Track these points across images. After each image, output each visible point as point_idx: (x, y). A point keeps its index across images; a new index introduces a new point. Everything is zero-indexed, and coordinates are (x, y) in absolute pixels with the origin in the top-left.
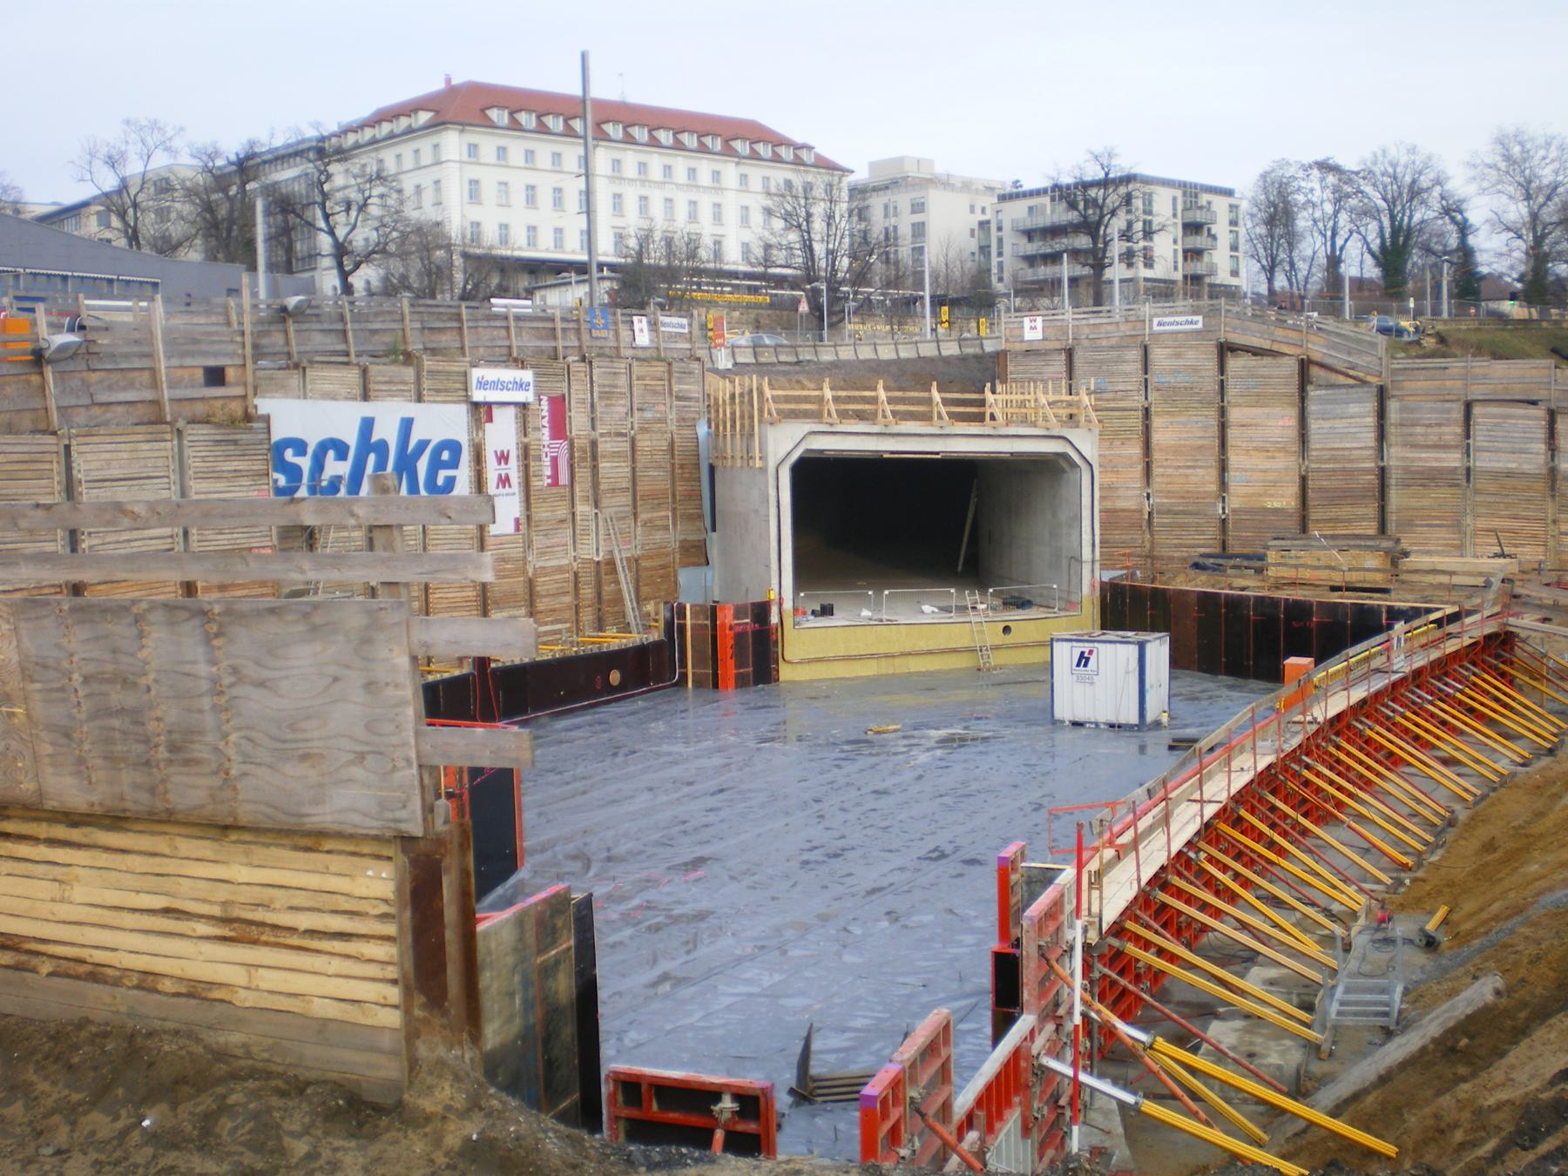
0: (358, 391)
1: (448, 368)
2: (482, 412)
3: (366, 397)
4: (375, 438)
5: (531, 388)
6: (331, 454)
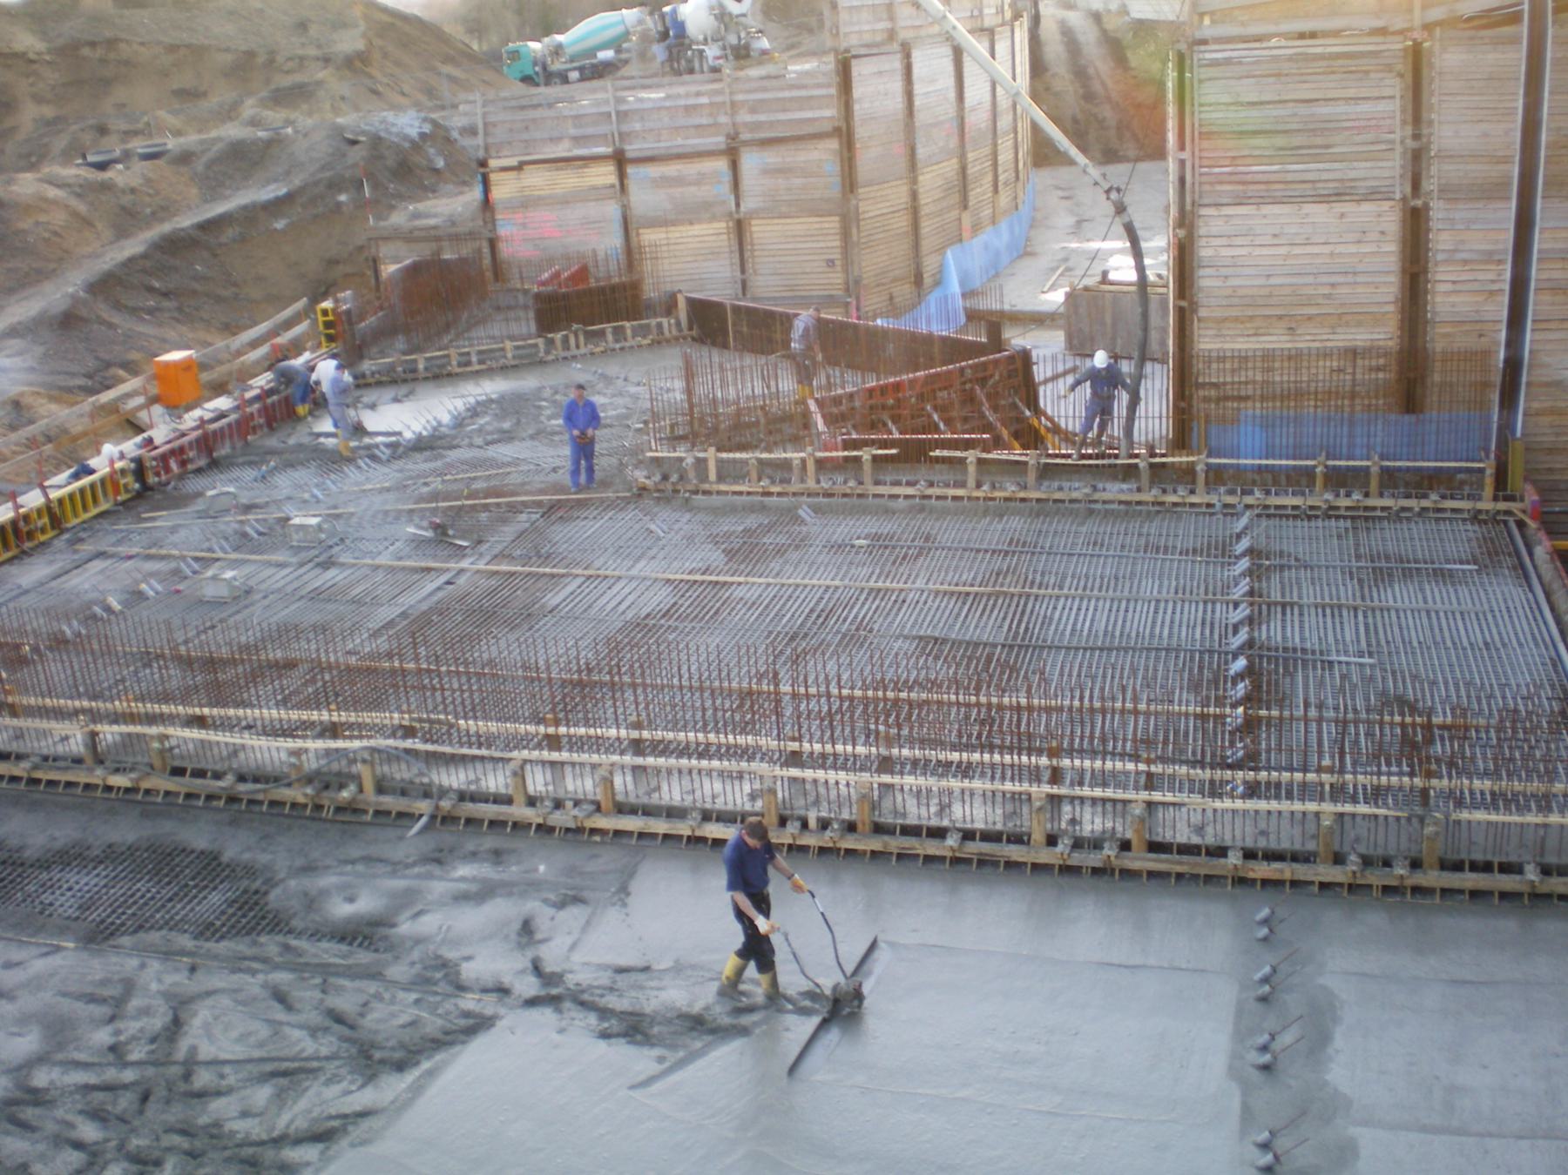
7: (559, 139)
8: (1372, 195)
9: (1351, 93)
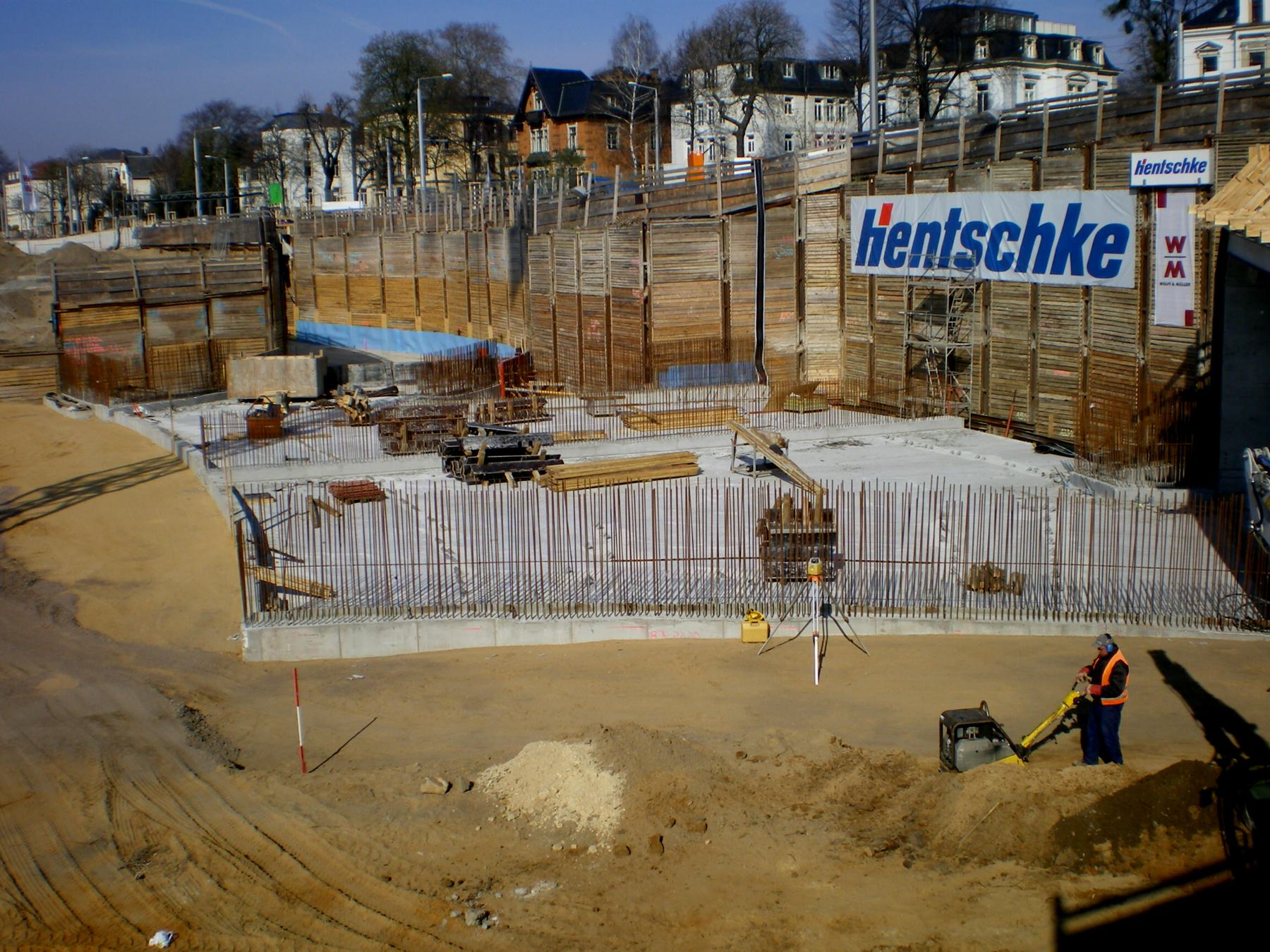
0: (1030, 182)
3: (1036, 187)
4: (1042, 221)
6: (1006, 235)
7: (101, 292)
8: (713, 279)
9: (703, 239)
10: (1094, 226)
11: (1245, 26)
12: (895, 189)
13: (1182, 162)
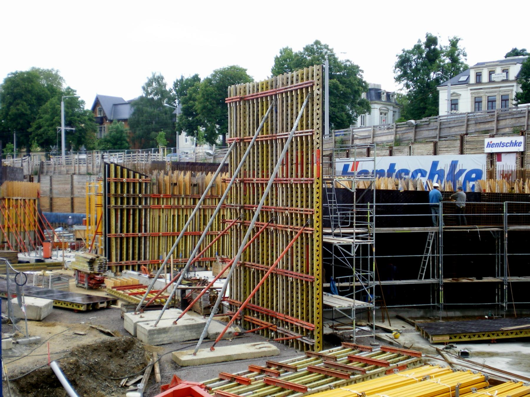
0: (432, 151)
1: (477, 139)
2: (493, 157)
3: (435, 153)
4: (438, 168)
5: (522, 145)
6: (419, 174)
10: (465, 170)
11: (473, 85)
12: (360, 154)
13: (510, 142)
